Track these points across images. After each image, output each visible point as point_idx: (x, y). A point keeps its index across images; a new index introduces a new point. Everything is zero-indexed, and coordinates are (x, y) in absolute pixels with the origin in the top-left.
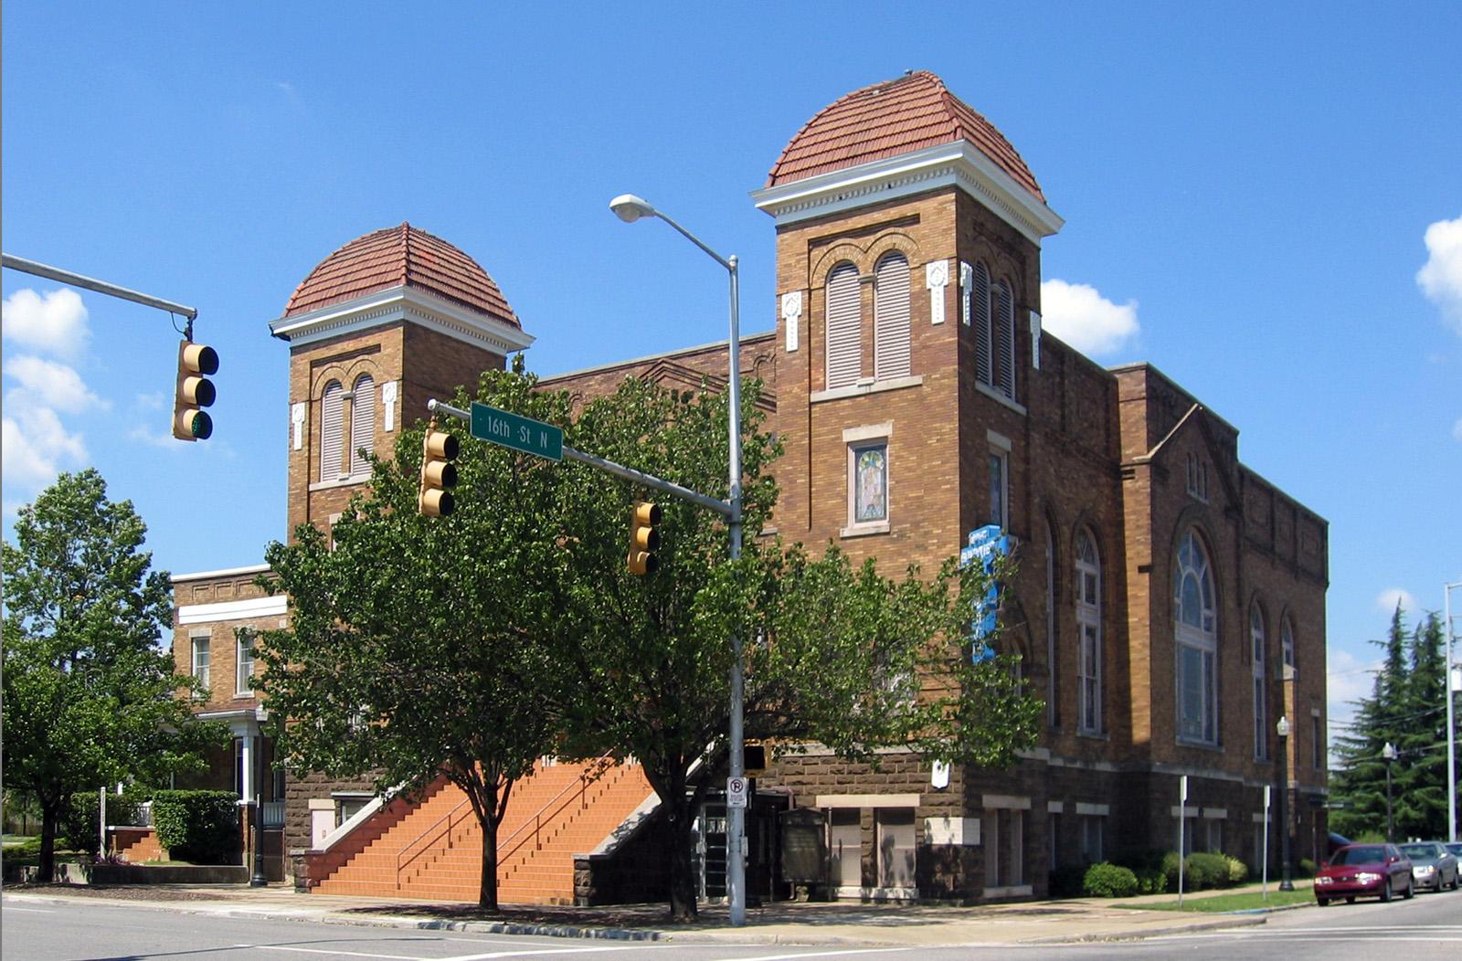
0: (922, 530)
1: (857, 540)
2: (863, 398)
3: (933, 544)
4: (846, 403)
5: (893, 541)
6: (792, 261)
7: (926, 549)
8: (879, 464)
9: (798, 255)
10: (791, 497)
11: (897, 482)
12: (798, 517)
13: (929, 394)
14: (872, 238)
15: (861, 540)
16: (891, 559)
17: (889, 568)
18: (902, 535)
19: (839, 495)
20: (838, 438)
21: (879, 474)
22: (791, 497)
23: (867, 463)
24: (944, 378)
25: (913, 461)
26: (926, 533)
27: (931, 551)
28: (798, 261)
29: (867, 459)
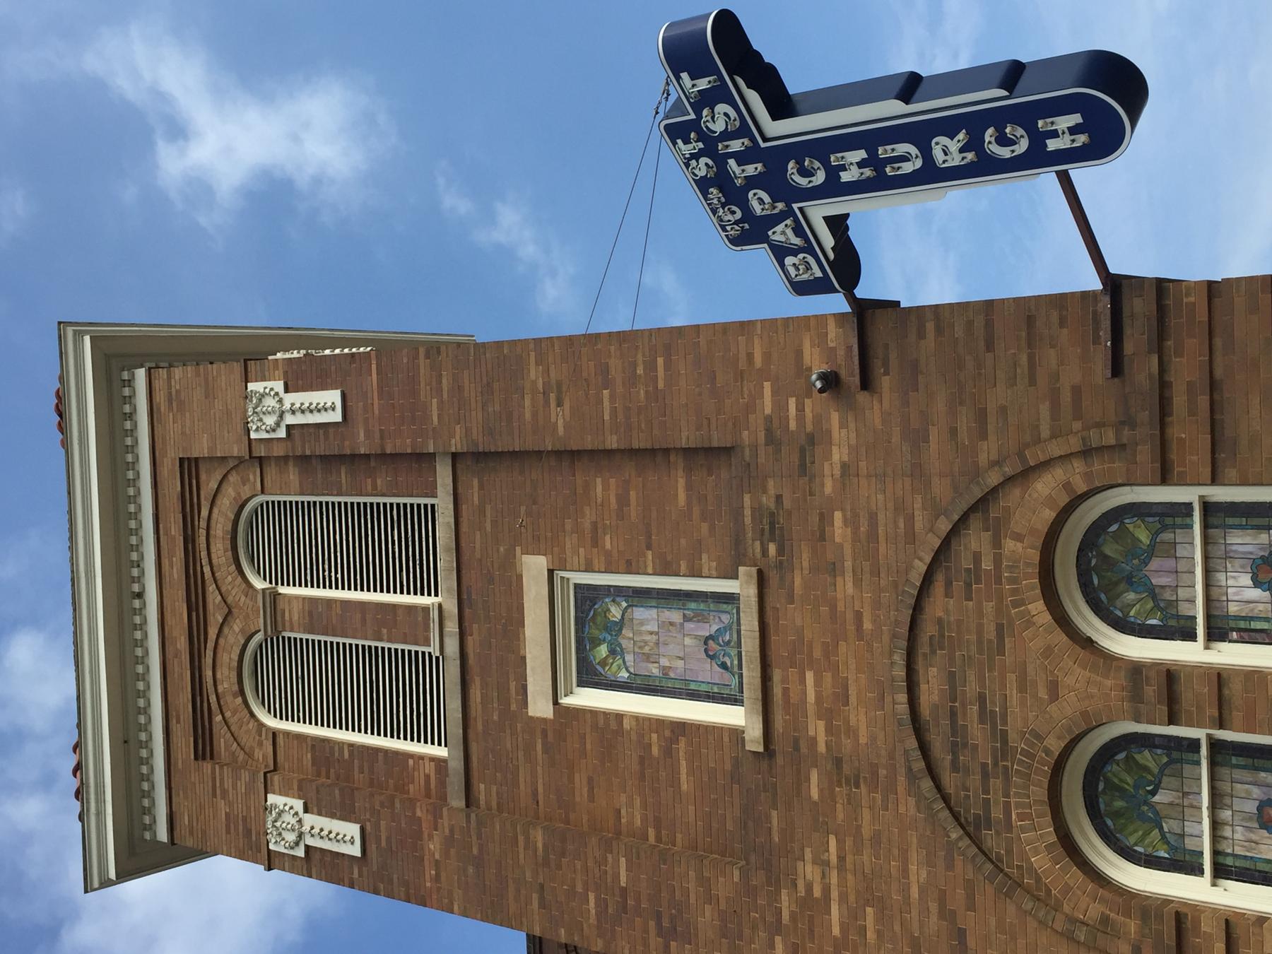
0: (761, 460)
1: (777, 690)
2: (470, 641)
3: (800, 409)
4: (476, 694)
5: (785, 565)
6: (222, 807)
7: (811, 439)
8: (615, 613)
9: (214, 795)
10: (659, 917)
11: (649, 547)
12: (709, 898)
13: (468, 432)
14: (213, 598)
15: (777, 675)
16: (834, 569)
17: (857, 582)
18: (772, 527)
19: (668, 752)
20: (544, 733)
21: (639, 613)
22: (659, 917)
23: (612, 652)
24: (440, 390)
25: (606, 488)
26: (771, 439)
27: (818, 420)
28: (224, 794)
29: (603, 650)
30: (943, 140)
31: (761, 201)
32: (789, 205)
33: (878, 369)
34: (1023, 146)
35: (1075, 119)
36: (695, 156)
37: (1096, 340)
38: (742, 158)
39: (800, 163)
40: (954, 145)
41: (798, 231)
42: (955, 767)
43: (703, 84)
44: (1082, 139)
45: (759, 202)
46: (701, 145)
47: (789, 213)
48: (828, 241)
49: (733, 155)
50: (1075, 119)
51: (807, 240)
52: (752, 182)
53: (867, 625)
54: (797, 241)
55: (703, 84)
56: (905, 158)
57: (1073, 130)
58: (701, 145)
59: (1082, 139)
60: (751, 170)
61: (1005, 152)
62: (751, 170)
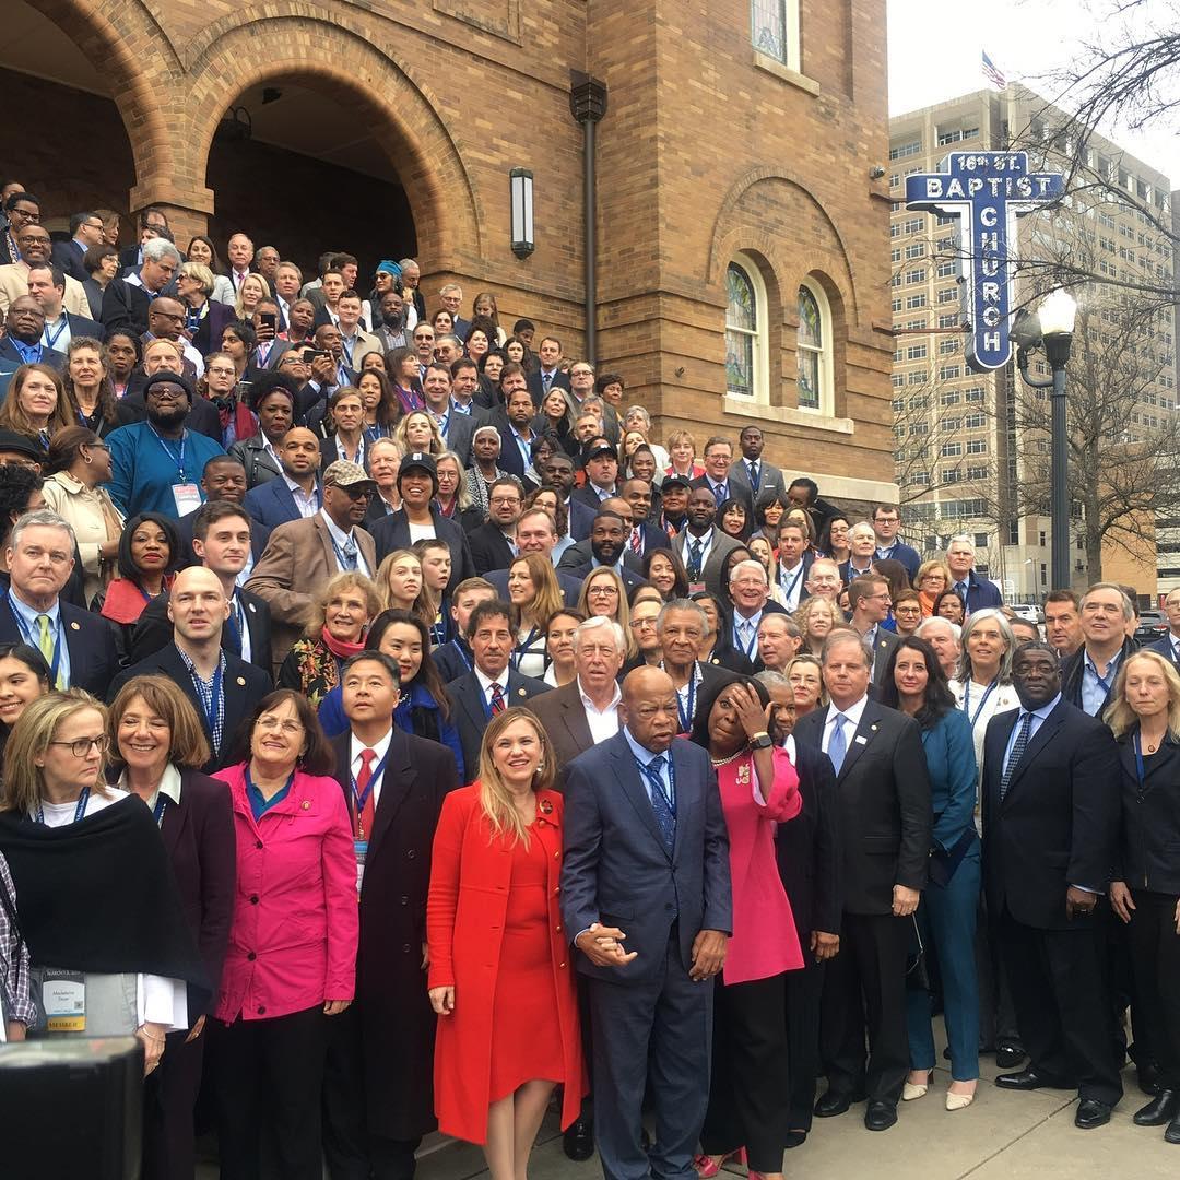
30: (996, 289)
31: (976, 185)
32: (971, 198)
33: (875, 204)
34: (986, 321)
35: (997, 349)
36: (1007, 162)
37: (882, 321)
38: (1001, 187)
39: (995, 216)
40: (993, 293)
41: (956, 196)
42: (759, 195)
43: (1043, 188)
44: (987, 347)
45: (976, 184)
46: (1012, 168)
47: (968, 197)
48: (947, 209)
49: (1004, 180)
50: (997, 349)
51: (949, 198)
52: (988, 186)
53: (801, 161)
54: (950, 193)
55: (1043, 188)
56: (991, 270)
57: (992, 346)
58: (1012, 168)
59: (987, 347)
60: (994, 189)
61: (986, 313)
62: (994, 189)
